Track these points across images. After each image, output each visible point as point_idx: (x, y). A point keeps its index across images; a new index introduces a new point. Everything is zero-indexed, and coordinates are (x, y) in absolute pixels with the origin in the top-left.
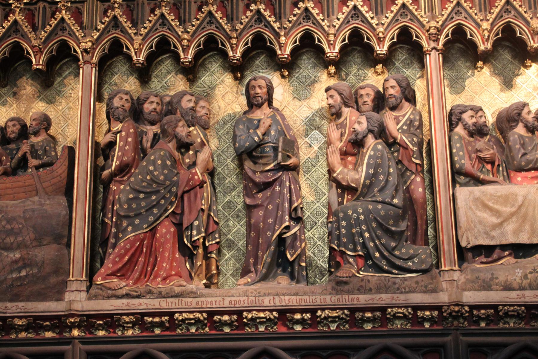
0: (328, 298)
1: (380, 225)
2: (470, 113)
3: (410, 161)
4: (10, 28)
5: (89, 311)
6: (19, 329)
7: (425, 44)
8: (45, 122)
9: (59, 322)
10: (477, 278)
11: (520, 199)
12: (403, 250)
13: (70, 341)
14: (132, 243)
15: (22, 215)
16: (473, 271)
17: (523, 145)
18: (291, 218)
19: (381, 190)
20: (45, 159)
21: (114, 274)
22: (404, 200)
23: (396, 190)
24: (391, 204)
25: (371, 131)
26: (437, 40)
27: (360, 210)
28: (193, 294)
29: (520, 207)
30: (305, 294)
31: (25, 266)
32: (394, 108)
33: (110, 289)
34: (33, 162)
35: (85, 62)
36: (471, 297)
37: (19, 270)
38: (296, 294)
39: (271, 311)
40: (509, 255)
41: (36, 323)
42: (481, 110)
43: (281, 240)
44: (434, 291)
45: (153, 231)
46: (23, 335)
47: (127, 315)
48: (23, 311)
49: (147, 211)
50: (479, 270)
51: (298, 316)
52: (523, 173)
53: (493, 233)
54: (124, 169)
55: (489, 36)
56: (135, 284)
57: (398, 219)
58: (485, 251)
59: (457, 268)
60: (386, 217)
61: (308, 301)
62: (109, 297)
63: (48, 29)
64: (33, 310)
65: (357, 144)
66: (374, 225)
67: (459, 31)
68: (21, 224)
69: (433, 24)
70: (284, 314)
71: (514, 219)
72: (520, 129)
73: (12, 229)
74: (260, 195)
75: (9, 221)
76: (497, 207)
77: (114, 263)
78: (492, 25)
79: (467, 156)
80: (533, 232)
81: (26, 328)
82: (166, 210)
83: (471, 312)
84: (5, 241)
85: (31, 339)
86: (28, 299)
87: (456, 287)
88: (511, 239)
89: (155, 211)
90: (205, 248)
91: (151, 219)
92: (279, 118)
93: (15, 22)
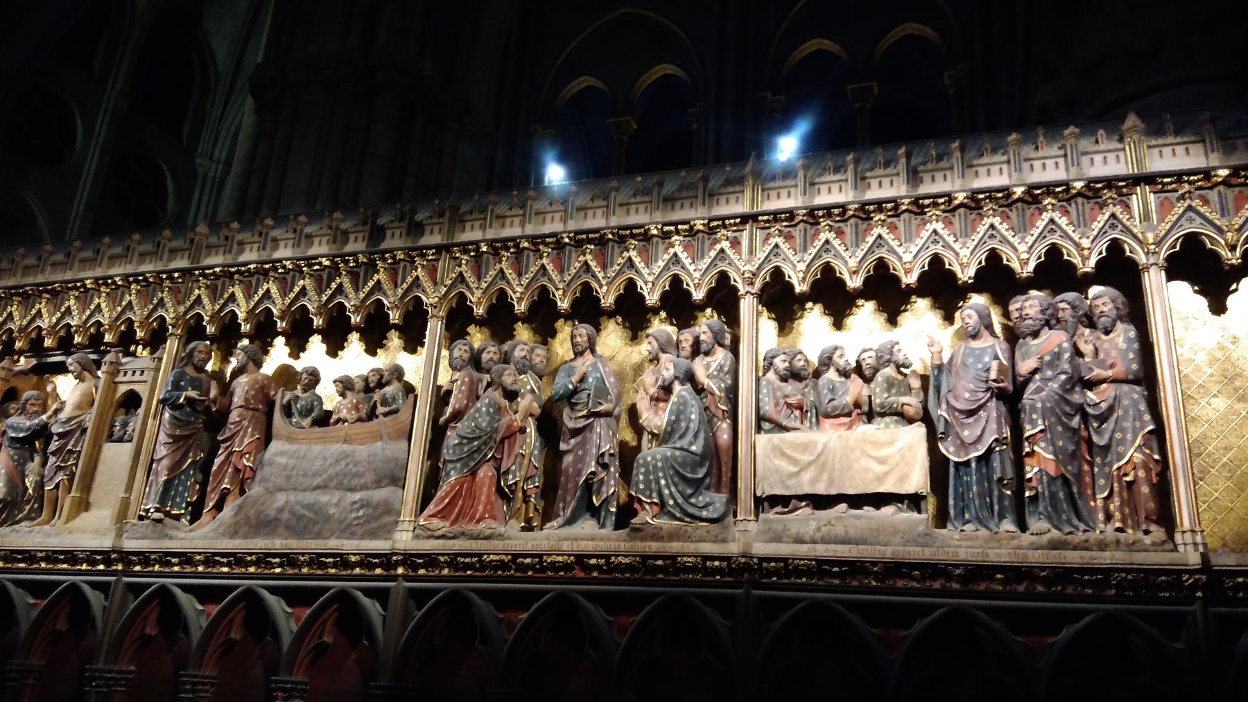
0: (622, 544)
1: (677, 472)
2: (782, 357)
3: (717, 407)
4: (336, 289)
7: (740, 286)
8: (398, 372)
9: (386, 560)
10: (769, 529)
11: (820, 447)
12: (701, 498)
13: (394, 578)
14: (453, 487)
16: (766, 521)
17: (832, 391)
18: (598, 462)
19: (681, 437)
20: (394, 406)
22: (704, 447)
23: (696, 436)
24: (688, 451)
25: (676, 378)
26: (752, 284)
27: (659, 457)
28: (500, 536)
29: (819, 456)
30: (601, 540)
31: (362, 507)
32: (707, 354)
34: (381, 410)
35: (433, 316)
36: (761, 549)
37: (358, 510)
38: (593, 539)
39: (569, 555)
40: (807, 506)
41: (367, 560)
42: (801, 353)
43: (589, 487)
44: (724, 541)
45: (473, 473)
46: (357, 571)
47: (443, 555)
50: (771, 521)
51: (593, 561)
52: (831, 420)
53: (789, 483)
54: (457, 416)
55: (804, 278)
56: (453, 524)
57: (695, 466)
58: (781, 501)
59: (753, 517)
60: (683, 465)
61: (603, 546)
62: (429, 537)
63: (405, 286)
65: (667, 389)
66: (671, 472)
67: (777, 273)
69: (748, 267)
70: (581, 558)
71: (812, 468)
72: (831, 374)
74: (572, 441)
75: (355, 465)
76: (795, 455)
77: (437, 505)
78: (809, 266)
79: (772, 404)
80: (831, 482)
81: (360, 564)
82: (486, 455)
83: (760, 564)
86: (362, 537)
87: (751, 537)
88: (807, 489)
89: (476, 455)
90: (524, 492)
91: (472, 464)
92: (600, 365)
93: (379, 281)
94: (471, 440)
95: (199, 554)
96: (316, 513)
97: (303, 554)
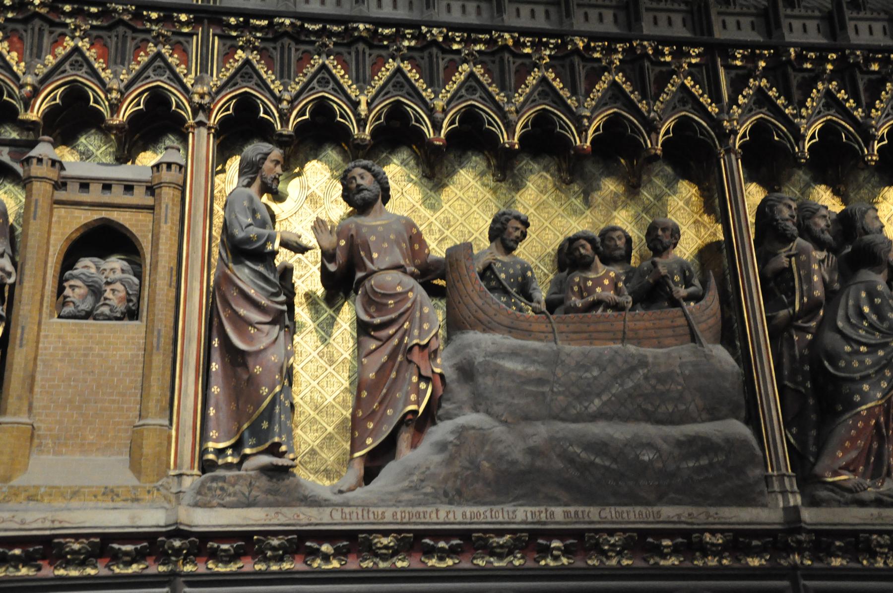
5: (821, 524)
6: (705, 550)
15: (678, 371)
21: (846, 468)
33: (849, 490)
46: (712, 562)
48: (717, 521)
49: (876, 372)
62: (847, 504)
64: (734, 520)
68: (680, 384)
73: (668, 391)
75: (662, 379)
84: (659, 410)
85: (726, 567)
86: (721, 502)
94: (873, 348)
95: (386, 533)
96: (615, 460)
97: (611, 532)
